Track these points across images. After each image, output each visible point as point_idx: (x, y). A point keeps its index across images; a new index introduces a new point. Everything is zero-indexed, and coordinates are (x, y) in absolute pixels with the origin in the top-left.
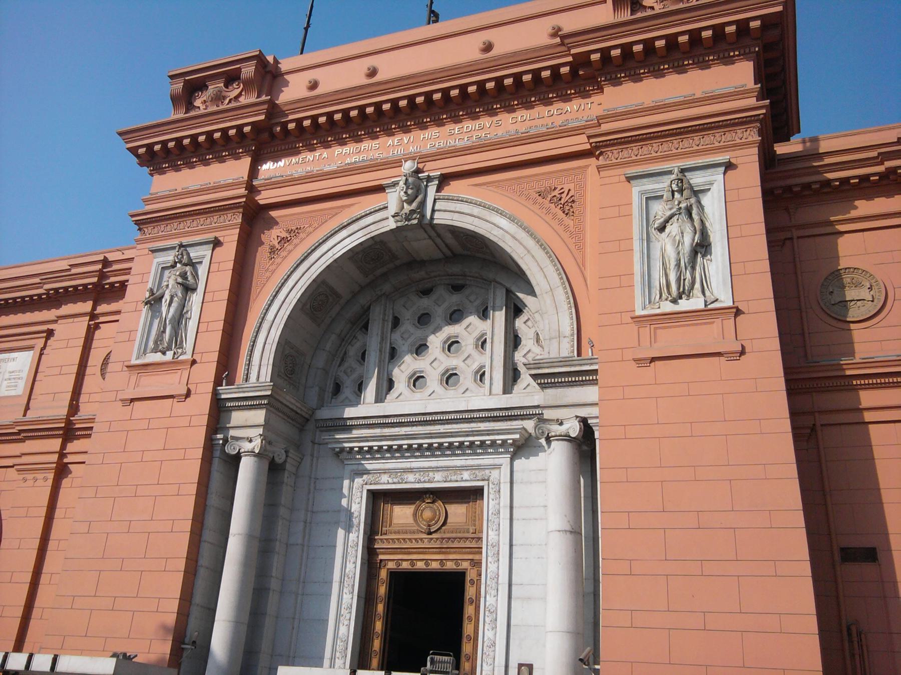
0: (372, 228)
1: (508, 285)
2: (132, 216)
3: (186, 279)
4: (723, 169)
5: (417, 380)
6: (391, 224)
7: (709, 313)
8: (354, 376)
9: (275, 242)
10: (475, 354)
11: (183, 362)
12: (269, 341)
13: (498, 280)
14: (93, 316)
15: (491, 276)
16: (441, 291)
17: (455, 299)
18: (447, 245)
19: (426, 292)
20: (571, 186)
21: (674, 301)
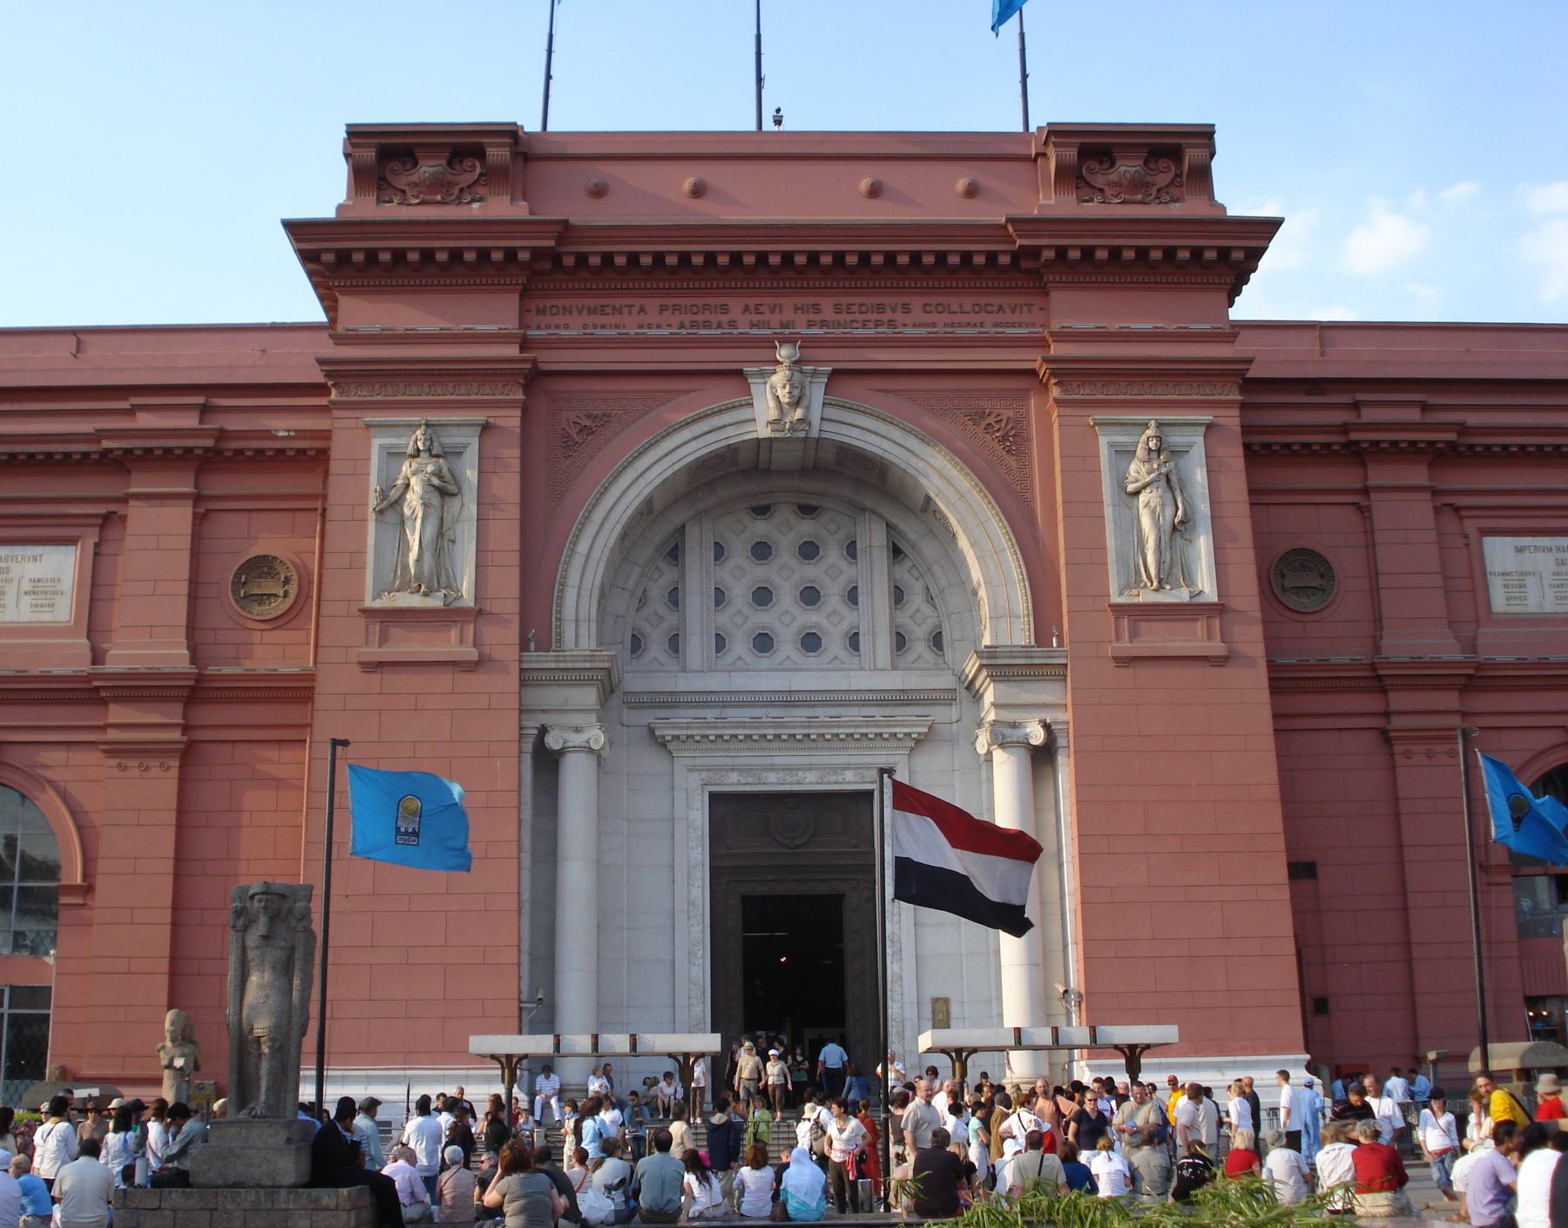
0: (730, 431)
1: (894, 520)
2: (321, 362)
4: (1202, 430)
5: (764, 642)
6: (764, 432)
7: (1193, 611)
8: (665, 626)
10: (843, 609)
11: (463, 612)
12: (587, 584)
13: (879, 510)
14: (198, 499)
15: (869, 503)
16: (785, 514)
17: (806, 528)
19: (762, 511)
20: (1011, 413)
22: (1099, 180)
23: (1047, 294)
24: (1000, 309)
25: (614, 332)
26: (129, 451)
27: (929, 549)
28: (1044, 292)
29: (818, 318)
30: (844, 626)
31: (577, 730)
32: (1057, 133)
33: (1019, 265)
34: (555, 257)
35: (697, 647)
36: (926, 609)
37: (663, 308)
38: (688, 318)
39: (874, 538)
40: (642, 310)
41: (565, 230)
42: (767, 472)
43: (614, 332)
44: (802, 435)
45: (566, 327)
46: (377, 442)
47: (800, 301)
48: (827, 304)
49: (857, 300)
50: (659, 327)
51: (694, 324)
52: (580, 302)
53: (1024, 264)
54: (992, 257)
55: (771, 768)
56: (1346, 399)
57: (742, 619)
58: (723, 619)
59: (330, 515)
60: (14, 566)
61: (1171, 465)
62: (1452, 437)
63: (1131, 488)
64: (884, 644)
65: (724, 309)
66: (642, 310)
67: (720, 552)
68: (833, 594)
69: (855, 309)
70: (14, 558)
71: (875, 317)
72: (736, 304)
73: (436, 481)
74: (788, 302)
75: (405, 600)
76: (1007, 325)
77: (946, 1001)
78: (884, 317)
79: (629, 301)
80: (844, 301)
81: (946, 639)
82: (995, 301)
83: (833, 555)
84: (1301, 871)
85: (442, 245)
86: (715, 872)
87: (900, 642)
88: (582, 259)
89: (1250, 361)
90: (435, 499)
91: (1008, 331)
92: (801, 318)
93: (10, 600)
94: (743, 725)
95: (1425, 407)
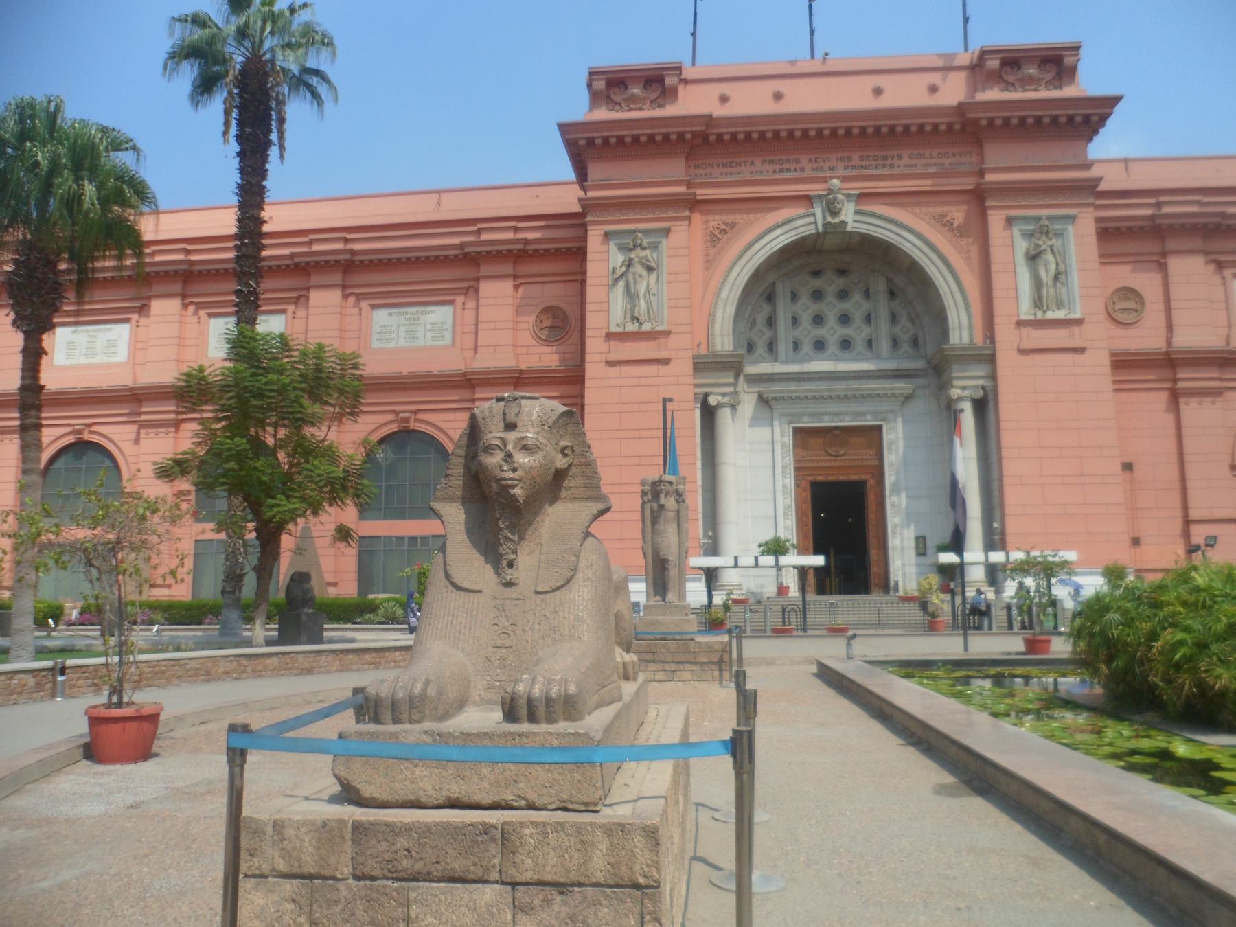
0: (802, 229)
9: (717, 232)
17: (840, 282)
19: (816, 273)
21: (1045, 312)
22: (1011, 78)
24: (954, 155)
26: (478, 253)
28: (979, 143)
29: (850, 164)
30: (863, 335)
31: (724, 395)
32: (984, 54)
33: (965, 129)
34: (705, 137)
35: (783, 347)
36: (909, 325)
37: (764, 162)
38: (778, 167)
39: (880, 286)
40: (752, 163)
41: (708, 120)
42: (820, 252)
46: (611, 243)
47: (840, 155)
51: (781, 171)
54: (950, 126)
55: (826, 414)
56: (1153, 200)
57: (807, 332)
58: (797, 333)
59: (589, 281)
60: (422, 317)
61: (1054, 241)
62: (1217, 220)
64: (884, 345)
65: (798, 161)
66: (752, 163)
67: (794, 297)
68: (858, 318)
70: (421, 313)
71: (882, 163)
72: (804, 160)
75: (631, 327)
77: (924, 538)
78: (890, 161)
81: (921, 342)
83: (857, 297)
84: (1128, 467)
85: (643, 132)
86: (796, 469)
87: (895, 343)
88: (720, 137)
89: (1099, 180)
90: (644, 273)
92: (841, 165)
93: (420, 334)
94: (811, 390)
95: (1200, 203)
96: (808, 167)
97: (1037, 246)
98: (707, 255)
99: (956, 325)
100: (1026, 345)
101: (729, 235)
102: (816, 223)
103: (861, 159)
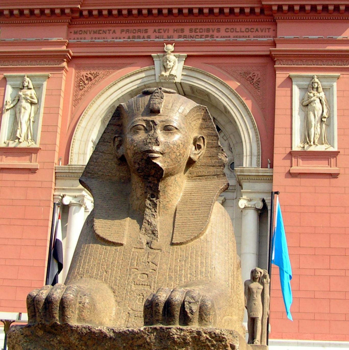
1: (215, 117)
3: (32, 97)
6: (158, 80)
18: (183, 91)
21: (311, 146)
23: (276, 24)
24: (257, 30)
25: (102, 40)
27: (228, 129)
29: (182, 34)
37: (122, 31)
38: (131, 35)
40: (114, 32)
43: (102, 40)
44: (172, 81)
45: (85, 39)
47: (176, 28)
48: (187, 29)
49: (199, 27)
50: (120, 38)
51: (134, 37)
52: (90, 29)
53: (266, 12)
54: (252, 10)
63: (305, 103)
69: (197, 31)
72: (151, 29)
73: (28, 97)
74: (171, 28)
76: (257, 37)
78: (209, 34)
79: (110, 28)
80: (194, 27)
82: (255, 27)
88: (90, 12)
91: (259, 39)
92: (176, 34)
96: (153, 35)
97: (309, 97)
98: (75, 96)
99: (248, 153)
100: (295, 169)
101: (93, 81)
102: (155, 75)
103: (191, 31)
